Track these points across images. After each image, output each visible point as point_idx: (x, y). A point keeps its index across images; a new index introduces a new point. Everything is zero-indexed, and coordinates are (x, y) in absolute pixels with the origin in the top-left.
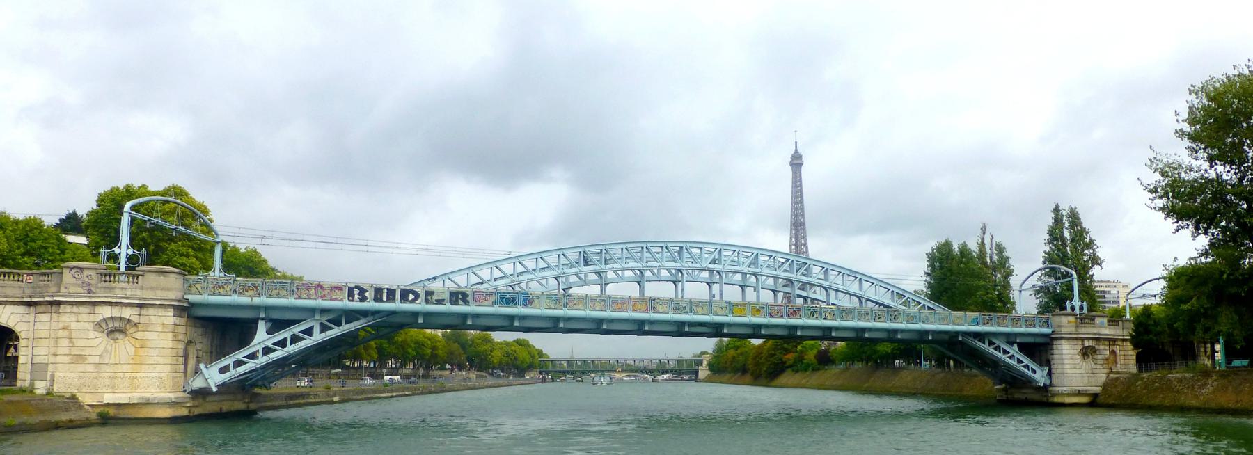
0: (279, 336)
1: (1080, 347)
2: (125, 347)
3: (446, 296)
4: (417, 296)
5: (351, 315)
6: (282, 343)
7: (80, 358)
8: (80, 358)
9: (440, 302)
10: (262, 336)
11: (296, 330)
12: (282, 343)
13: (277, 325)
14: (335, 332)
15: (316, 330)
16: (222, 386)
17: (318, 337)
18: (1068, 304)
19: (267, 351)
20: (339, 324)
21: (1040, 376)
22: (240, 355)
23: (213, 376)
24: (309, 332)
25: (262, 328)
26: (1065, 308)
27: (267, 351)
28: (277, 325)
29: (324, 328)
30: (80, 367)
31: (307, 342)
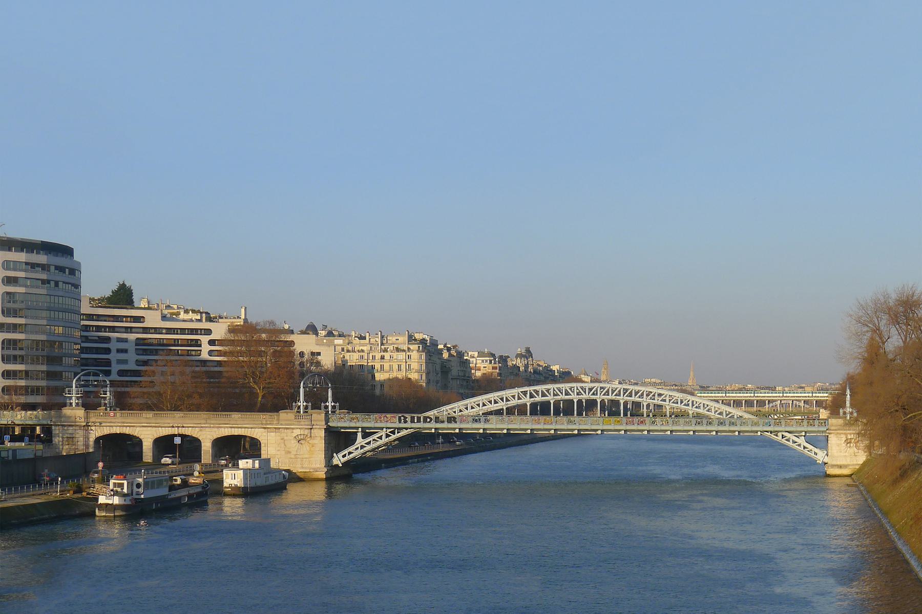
0: (367, 440)
1: (844, 439)
2: (305, 447)
3: (445, 419)
4: (431, 419)
5: (400, 429)
6: (369, 443)
7: (289, 452)
8: (289, 452)
9: (443, 422)
10: (360, 440)
11: (375, 437)
12: (369, 443)
13: (366, 435)
14: (393, 437)
15: (384, 437)
16: (344, 464)
17: (385, 440)
18: (841, 411)
19: (362, 447)
20: (393, 433)
21: (820, 456)
22: (351, 449)
23: (339, 459)
24: (380, 438)
25: (359, 435)
26: (839, 414)
27: (362, 447)
28: (366, 435)
29: (387, 436)
30: (289, 456)
31: (380, 442)
